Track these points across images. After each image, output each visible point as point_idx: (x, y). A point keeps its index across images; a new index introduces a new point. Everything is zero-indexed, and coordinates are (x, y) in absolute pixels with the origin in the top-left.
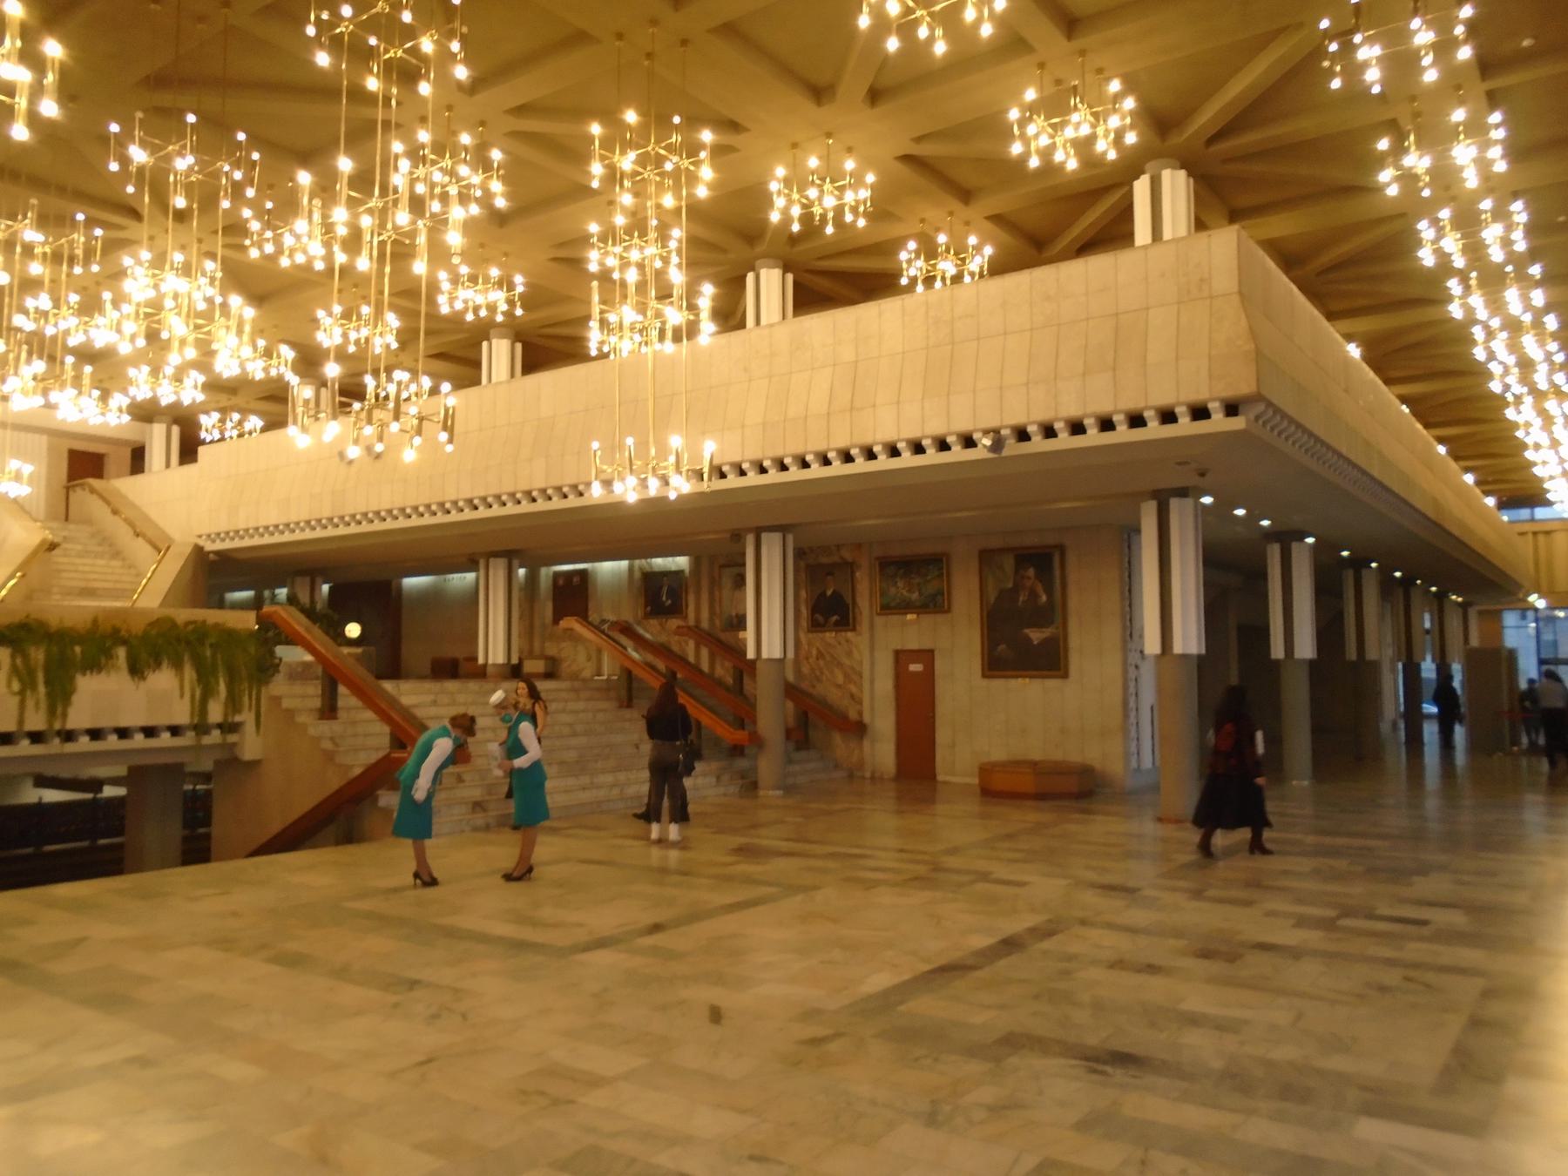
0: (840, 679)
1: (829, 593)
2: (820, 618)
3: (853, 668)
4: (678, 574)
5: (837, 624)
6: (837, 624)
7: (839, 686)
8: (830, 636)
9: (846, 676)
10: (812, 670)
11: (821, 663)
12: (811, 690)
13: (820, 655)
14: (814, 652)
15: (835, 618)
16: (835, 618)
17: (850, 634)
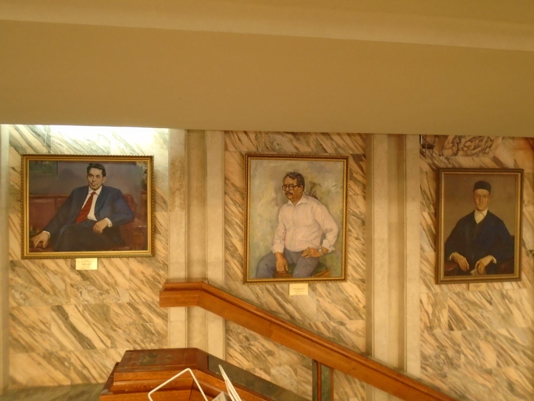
0: (490, 359)
1: (479, 217)
2: (462, 261)
3: (513, 341)
4: (136, 165)
5: (491, 269)
6: (491, 269)
7: (489, 372)
8: (476, 292)
9: (501, 353)
10: (442, 347)
11: (457, 334)
12: (438, 383)
13: (455, 322)
14: (445, 317)
15: (487, 260)
16: (487, 260)
17: (507, 286)
